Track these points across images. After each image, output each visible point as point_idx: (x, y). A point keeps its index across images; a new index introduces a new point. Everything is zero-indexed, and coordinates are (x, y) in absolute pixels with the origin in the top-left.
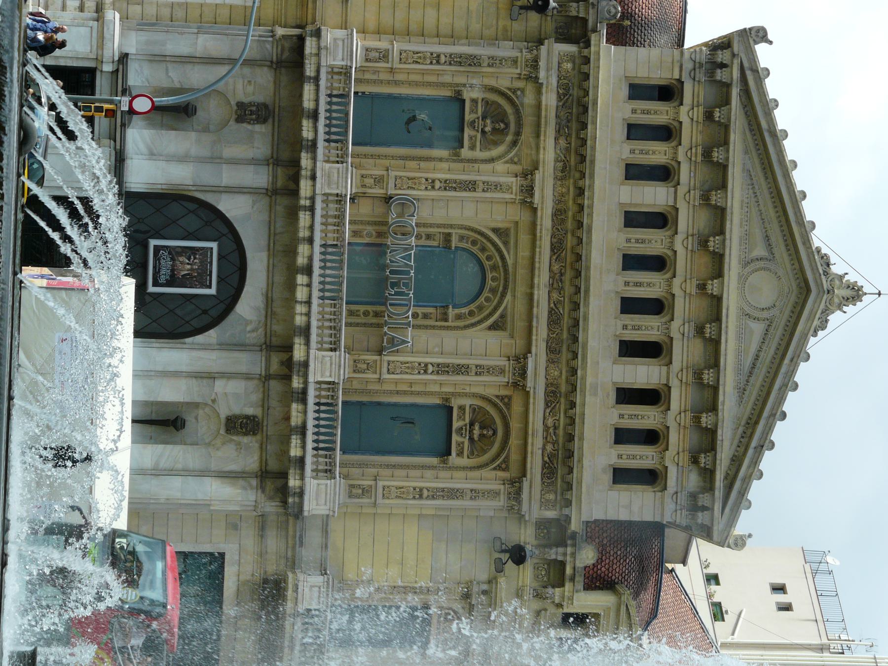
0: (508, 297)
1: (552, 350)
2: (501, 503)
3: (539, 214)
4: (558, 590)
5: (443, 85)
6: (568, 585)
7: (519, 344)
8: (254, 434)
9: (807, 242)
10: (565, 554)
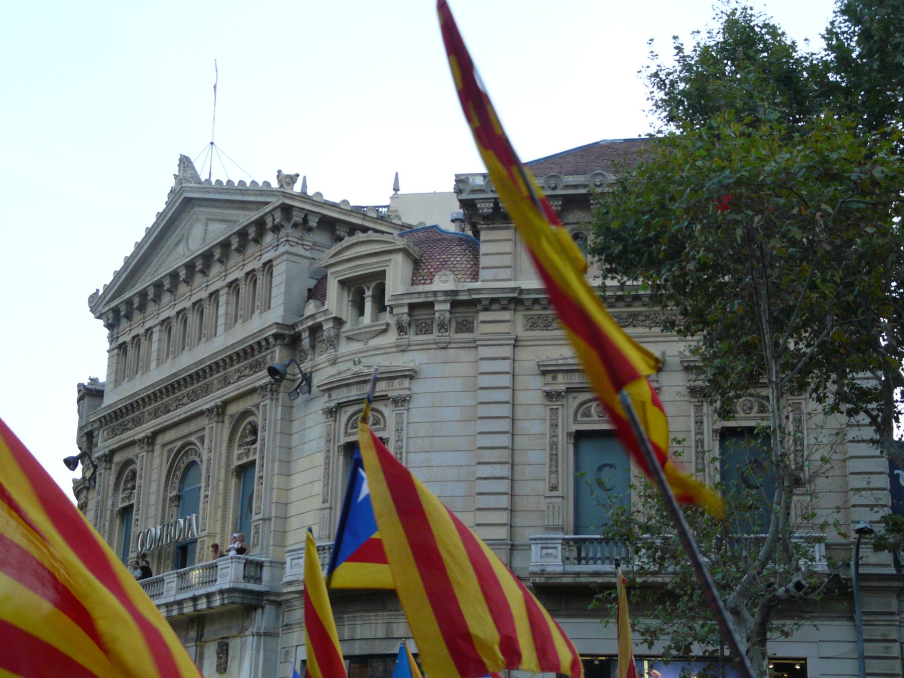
0: (192, 439)
1: (207, 390)
2: (268, 402)
3: (152, 430)
4: (326, 327)
6: (319, 320)
8: (227, 645)
10: (304, 330)
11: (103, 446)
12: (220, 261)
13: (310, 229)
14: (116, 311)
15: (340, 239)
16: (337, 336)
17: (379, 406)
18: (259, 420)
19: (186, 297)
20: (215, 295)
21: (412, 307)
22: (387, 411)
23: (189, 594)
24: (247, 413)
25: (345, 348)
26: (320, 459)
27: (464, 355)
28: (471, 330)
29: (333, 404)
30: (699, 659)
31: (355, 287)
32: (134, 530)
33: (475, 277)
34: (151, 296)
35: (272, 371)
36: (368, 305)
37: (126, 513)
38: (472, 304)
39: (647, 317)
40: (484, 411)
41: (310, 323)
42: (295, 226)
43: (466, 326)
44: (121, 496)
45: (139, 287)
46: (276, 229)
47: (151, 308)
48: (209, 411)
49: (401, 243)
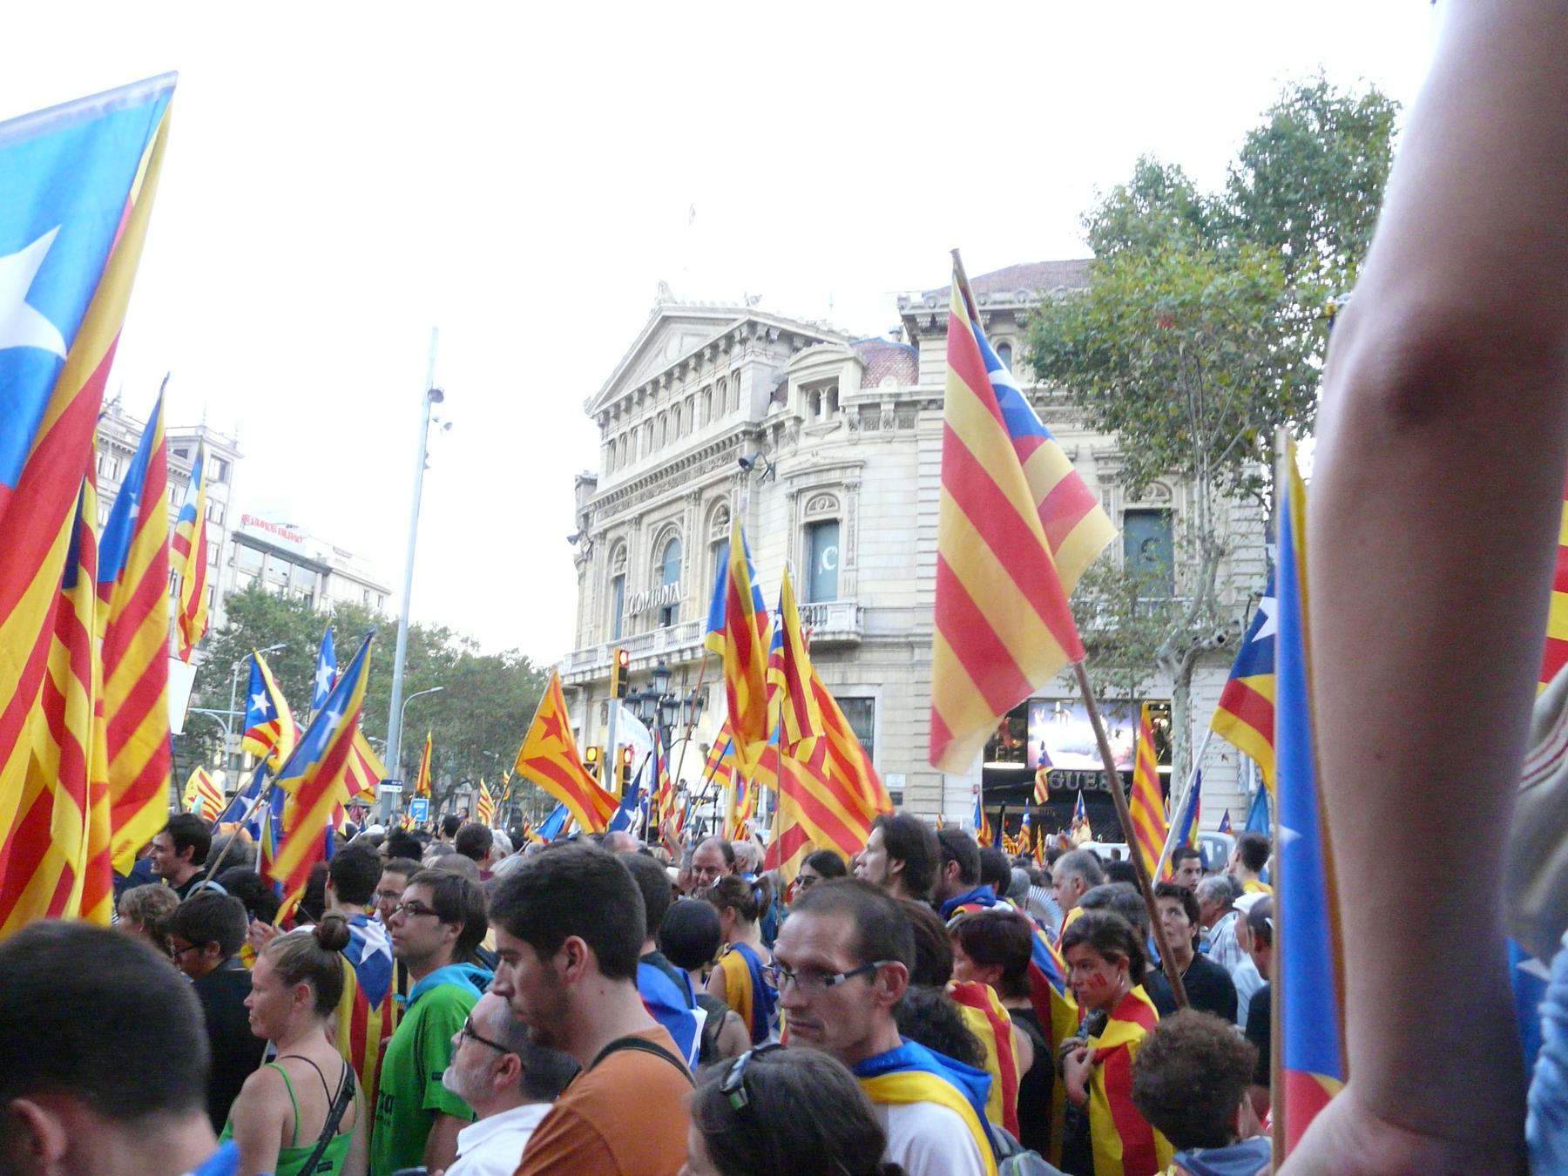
0: (673, 519)
1: (685, 478)
5: (607, 593)
7: (682, 505)
9: (646, 330)
11: (598, 524)
12: (695, 369)
13: (772, 342)
14: (606, 413)
15: (797, 350)
16: (797, 432)
17: (834, 491)
18: (730, 503)
19: (665, 400)
20: (690, 398)
21: (861, 407)
22: (840, 494)
23: (676, 648)
24: (720, 498)
25: (804, 442)
26: (784, 535)
27: (908, 448)
28: (911, 426)
29: (794, 490)
30: (1113, 701)
31: (812, 391)
32: (627, 595)
33: (915, 381)
34: (635, 399)
35: (743, 462)
36: (824, 405)
37: (619, 580)
38: (914, 404)
39: (1063, 414)
40: (923, 495)
41: (774, 421)
42: (760, 338)
43: (907, 423)
44: (614, 566)
45: (625, 393)
46: (743, 341)
47: (636, 409)
48: (689, 496)
49: (851, 353)
